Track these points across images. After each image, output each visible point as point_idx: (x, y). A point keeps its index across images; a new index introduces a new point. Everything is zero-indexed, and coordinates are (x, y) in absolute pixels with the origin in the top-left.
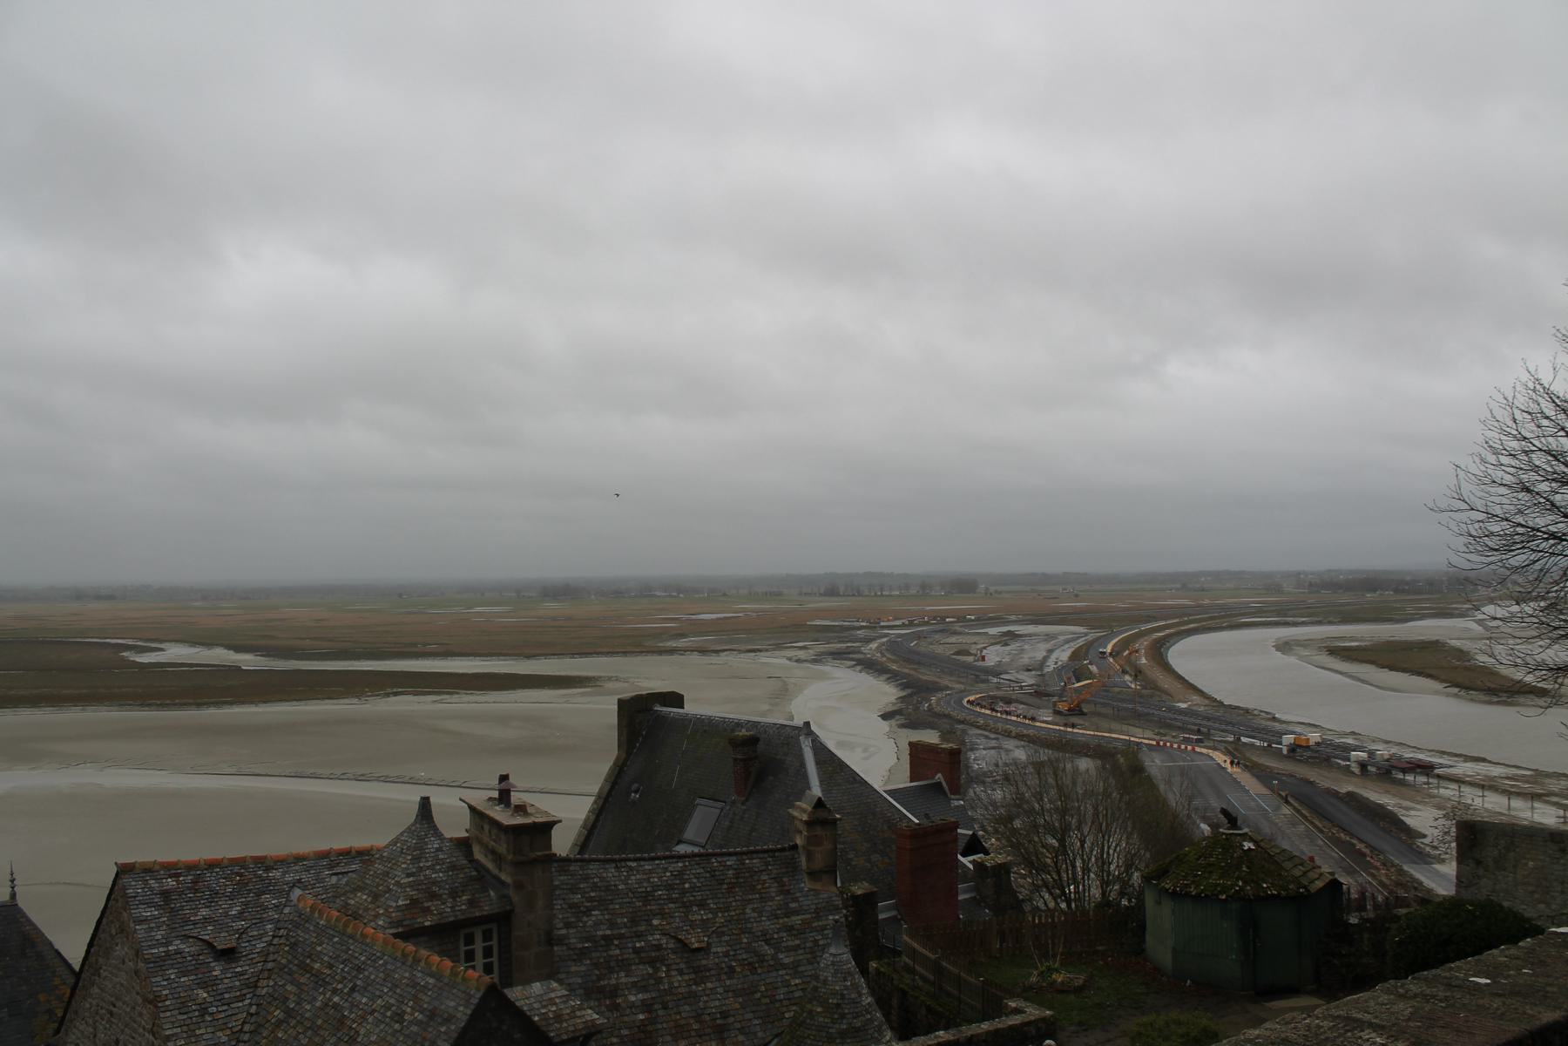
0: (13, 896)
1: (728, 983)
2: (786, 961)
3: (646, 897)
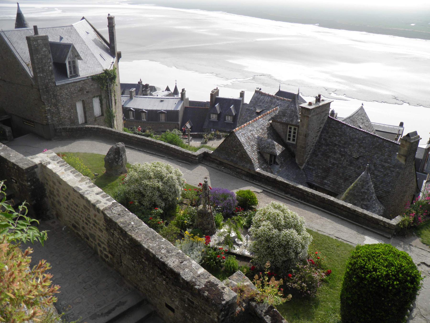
0: (299, 93)
1: (356, 170)
2: (376, 173)
3: (352, 139)
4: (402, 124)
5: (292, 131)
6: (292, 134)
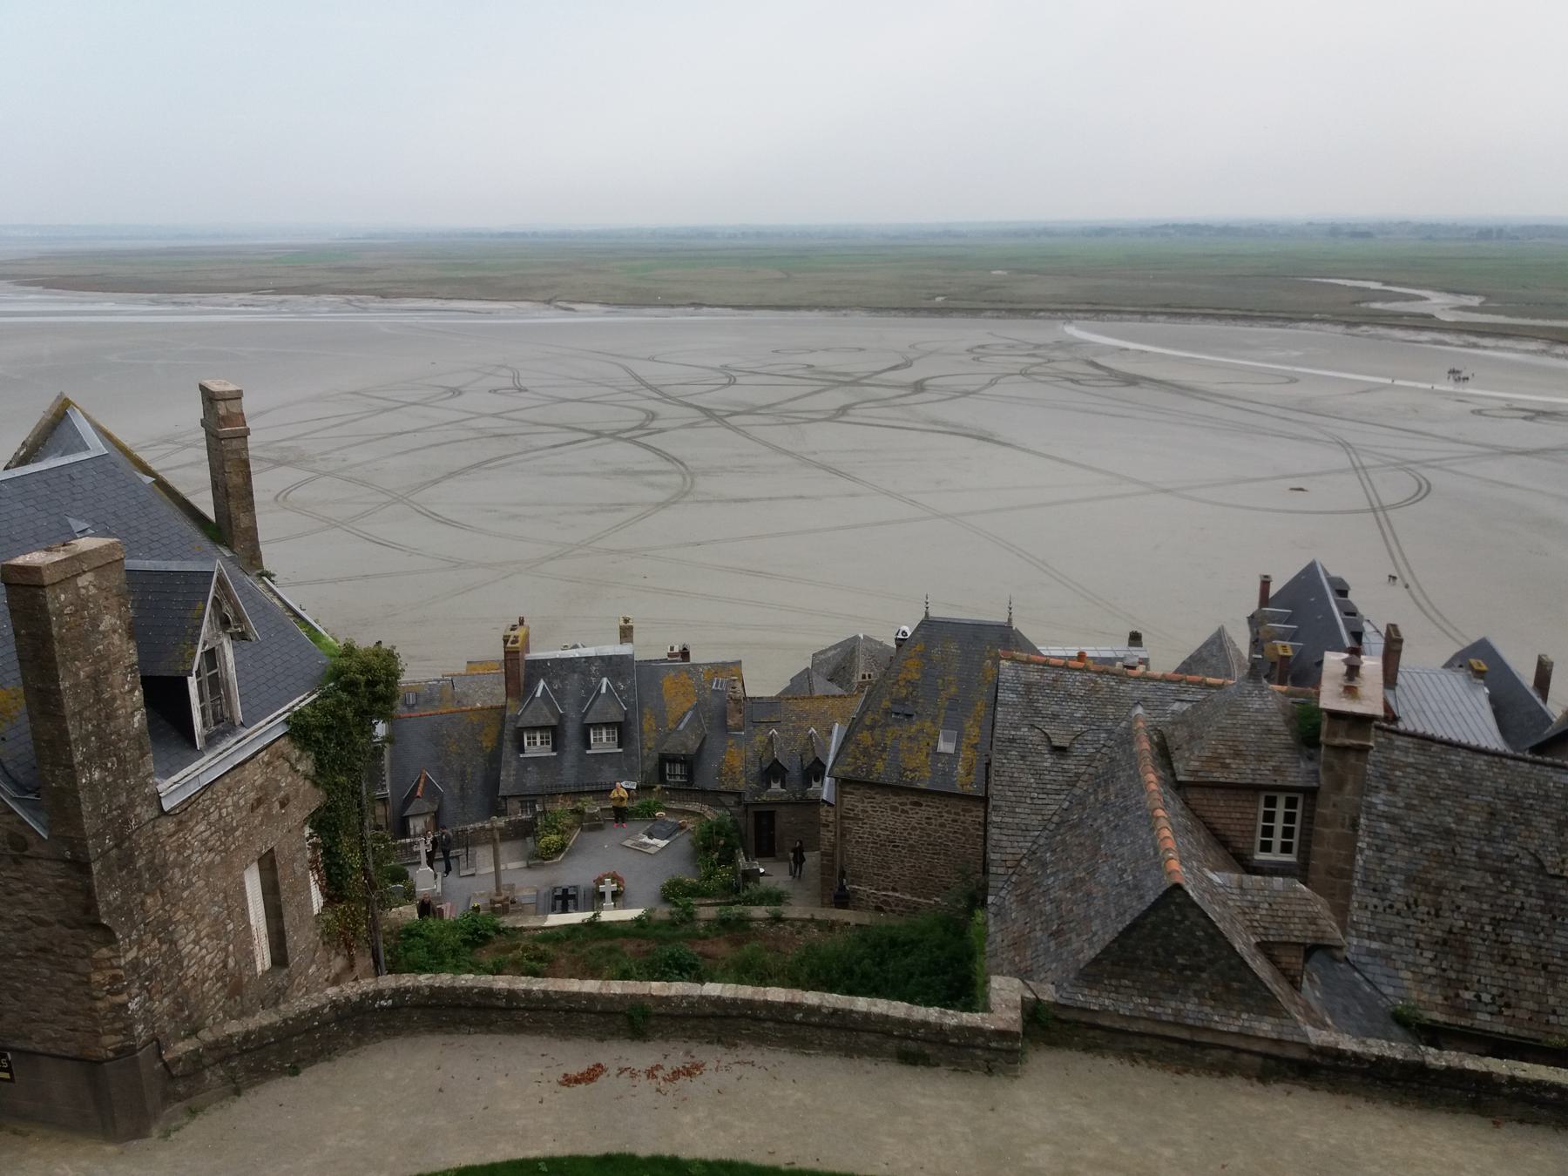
0: (1010, 620)
4: (1135, 639)
5: (1280, 810)
6: (1279, 825)
